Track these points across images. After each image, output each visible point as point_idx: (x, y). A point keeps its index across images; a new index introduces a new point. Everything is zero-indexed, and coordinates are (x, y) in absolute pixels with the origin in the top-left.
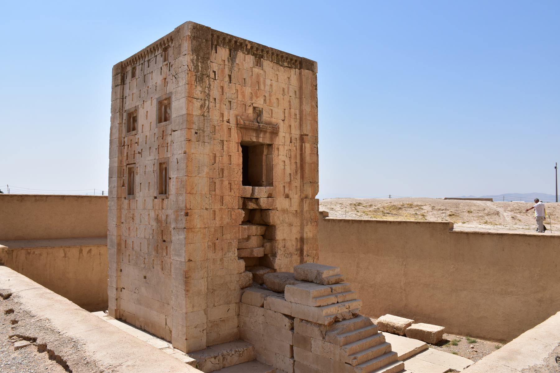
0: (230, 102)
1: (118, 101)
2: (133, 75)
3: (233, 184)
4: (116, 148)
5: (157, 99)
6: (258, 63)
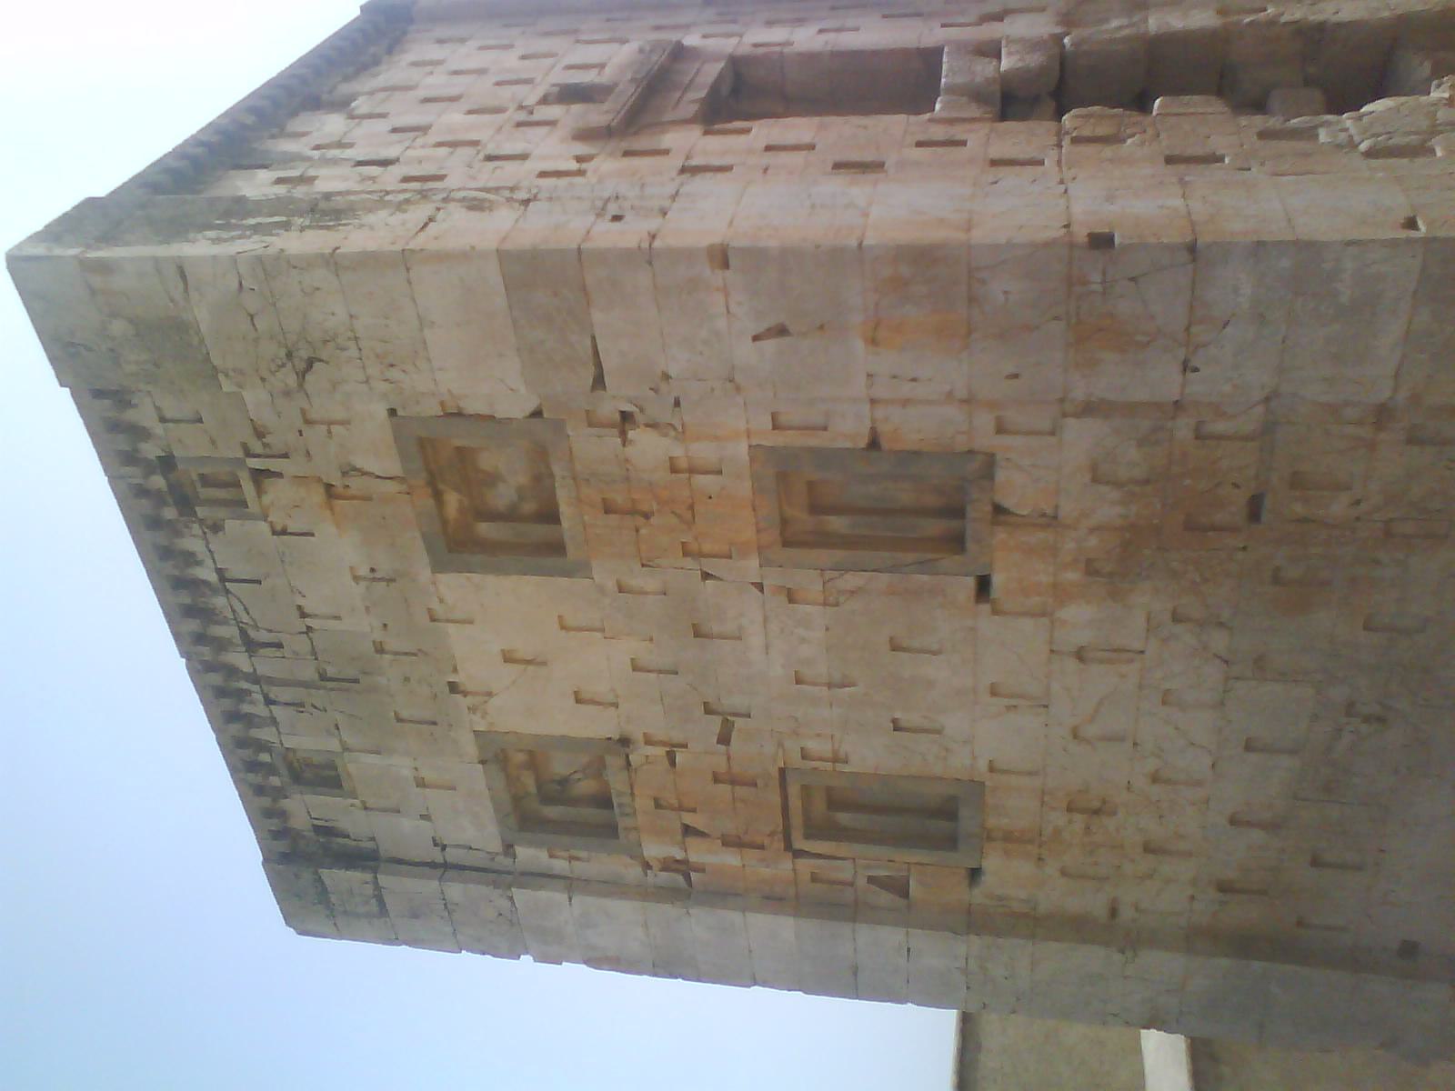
0: (490, 158)
1: (455, 890)
2: (326, 777)
3: (921, 137)
4: (698, 925)
5: (439, 566)
6: (342, 105)
